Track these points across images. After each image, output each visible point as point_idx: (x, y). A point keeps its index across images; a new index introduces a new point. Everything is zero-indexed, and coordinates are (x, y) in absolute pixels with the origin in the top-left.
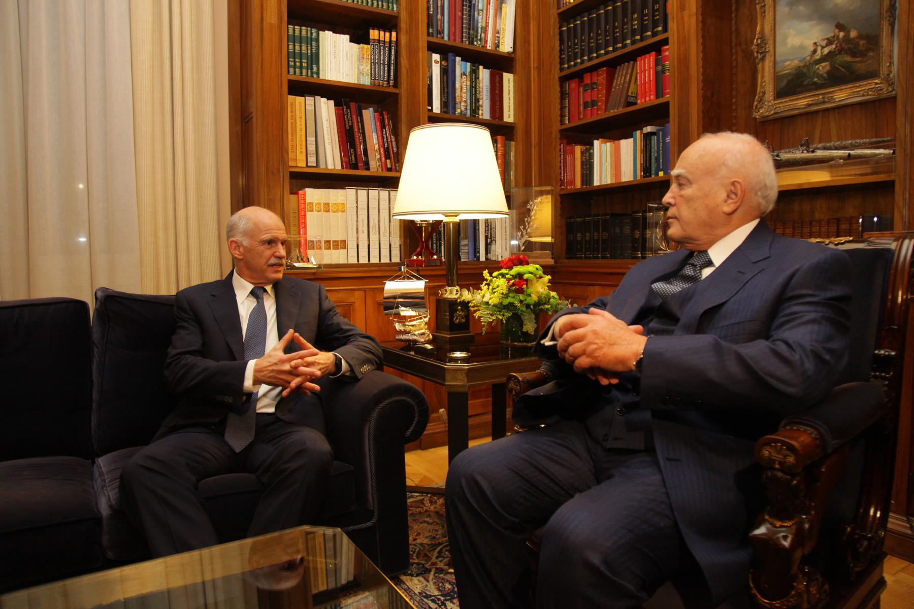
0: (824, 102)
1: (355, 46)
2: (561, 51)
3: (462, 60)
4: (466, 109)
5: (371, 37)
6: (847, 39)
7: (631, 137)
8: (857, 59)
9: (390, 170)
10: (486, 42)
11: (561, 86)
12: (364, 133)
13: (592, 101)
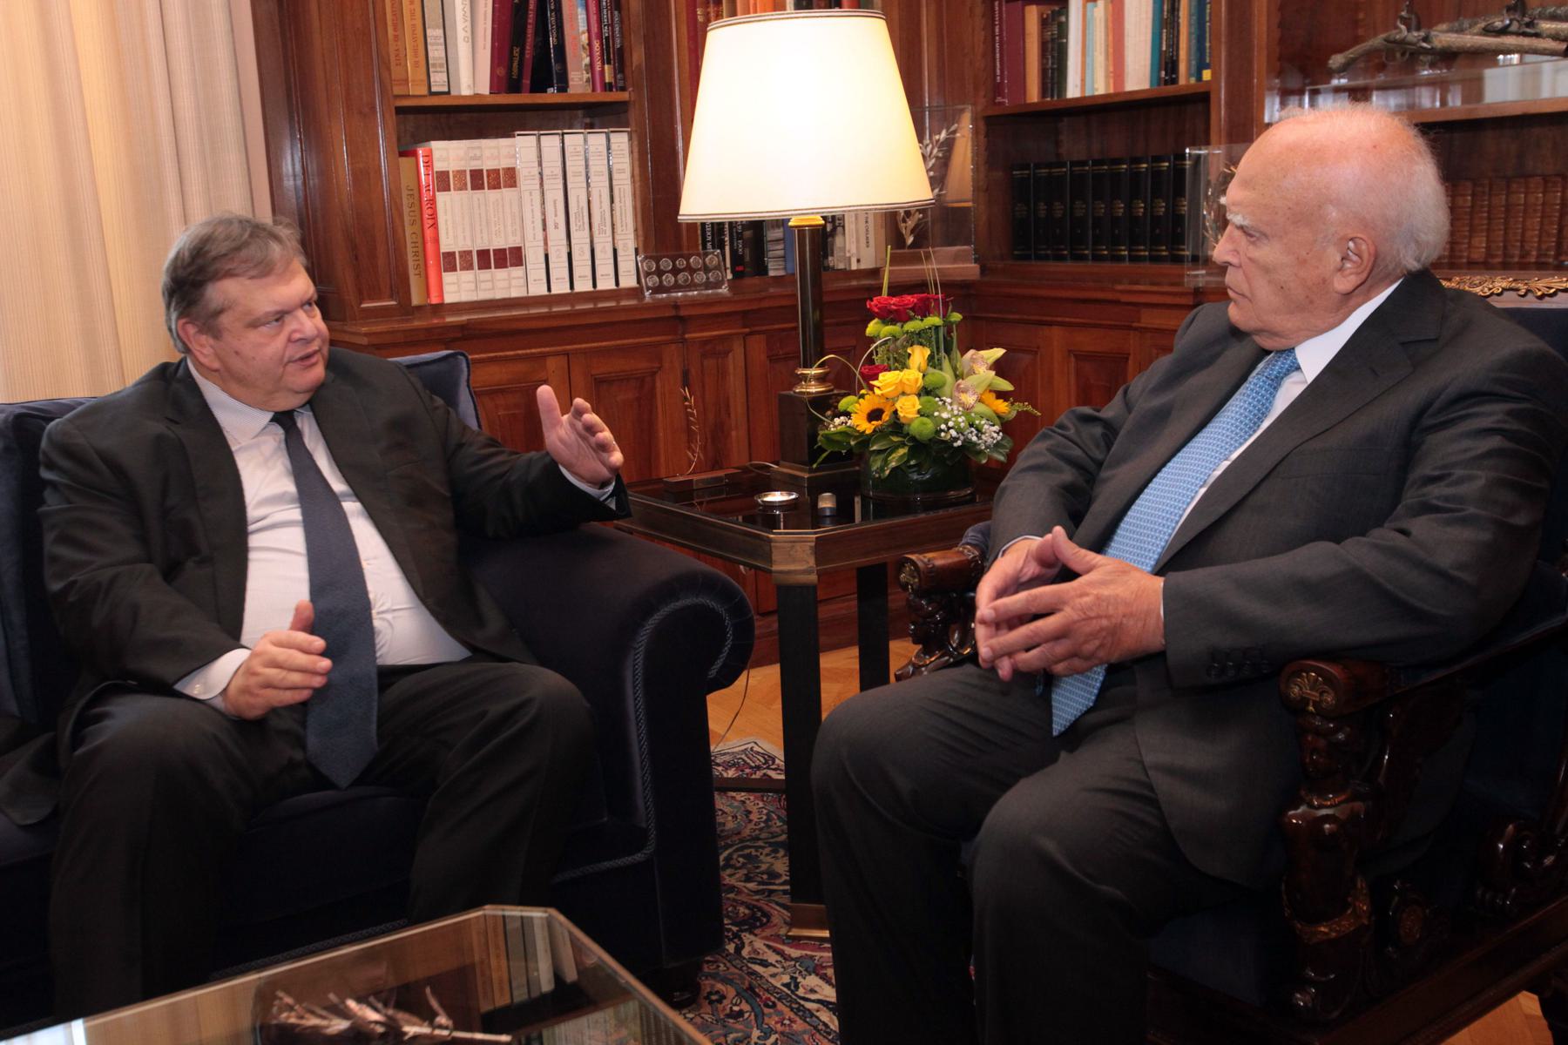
9: (608, 87)
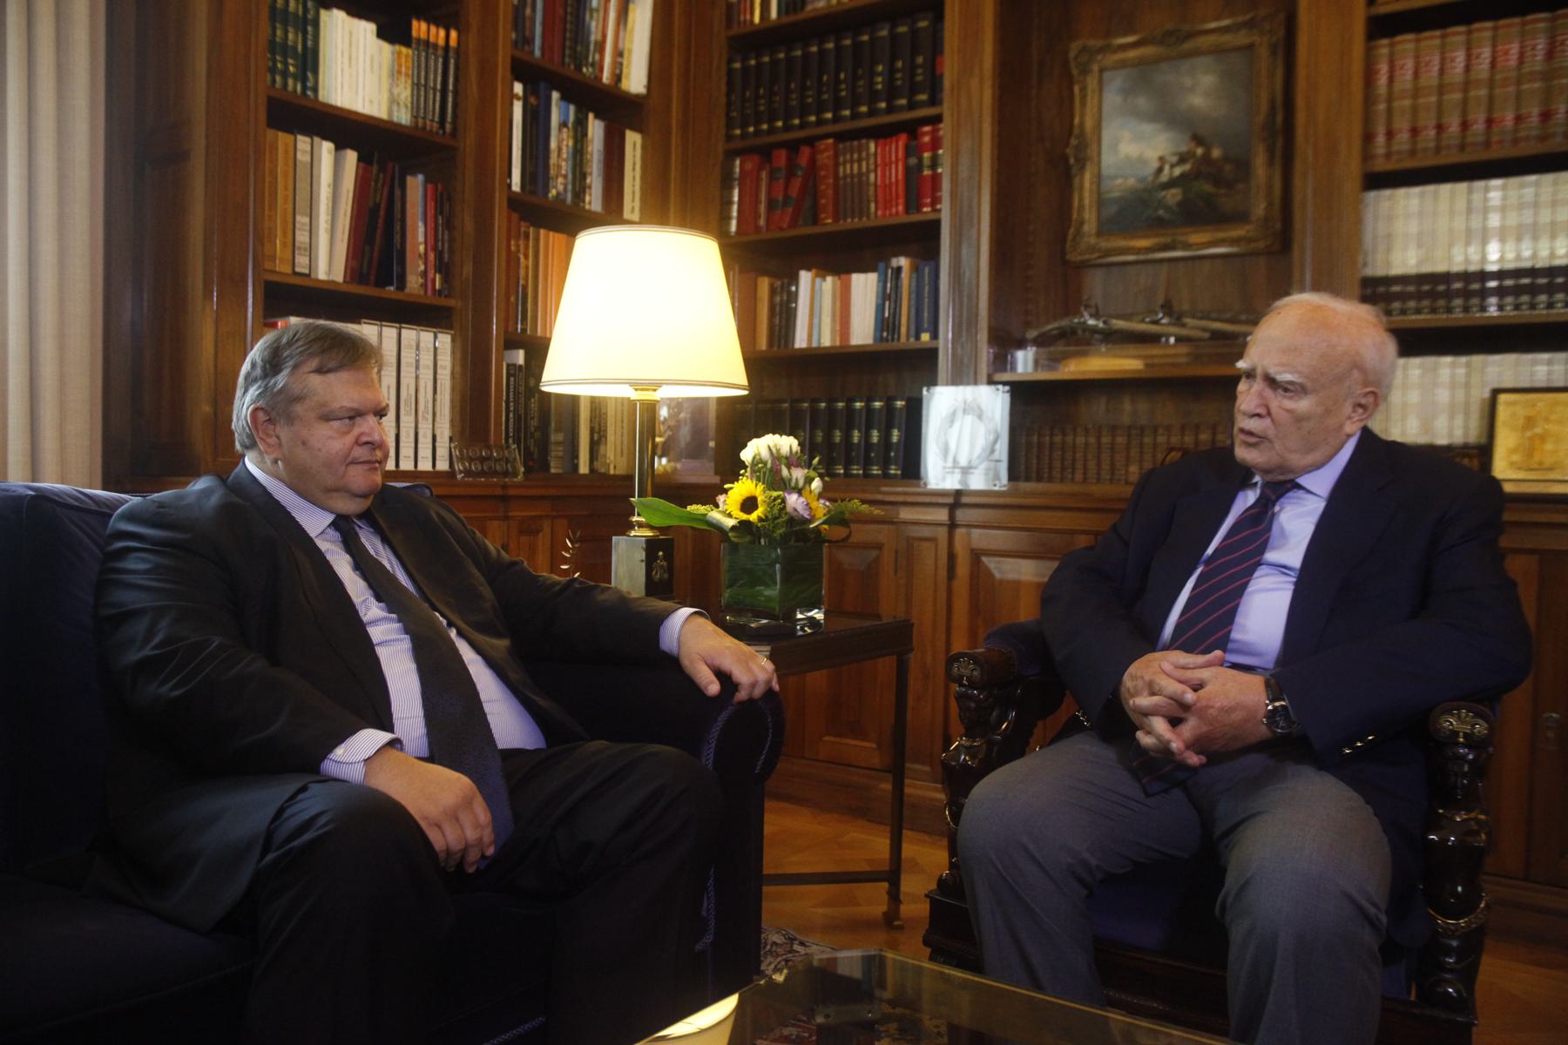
1: (387, 48)
2: (729, 104)
3: (564, 98)
5: (414, 34)
6: (1206, 157)
8: (1223, 191)
10: (601, 70)
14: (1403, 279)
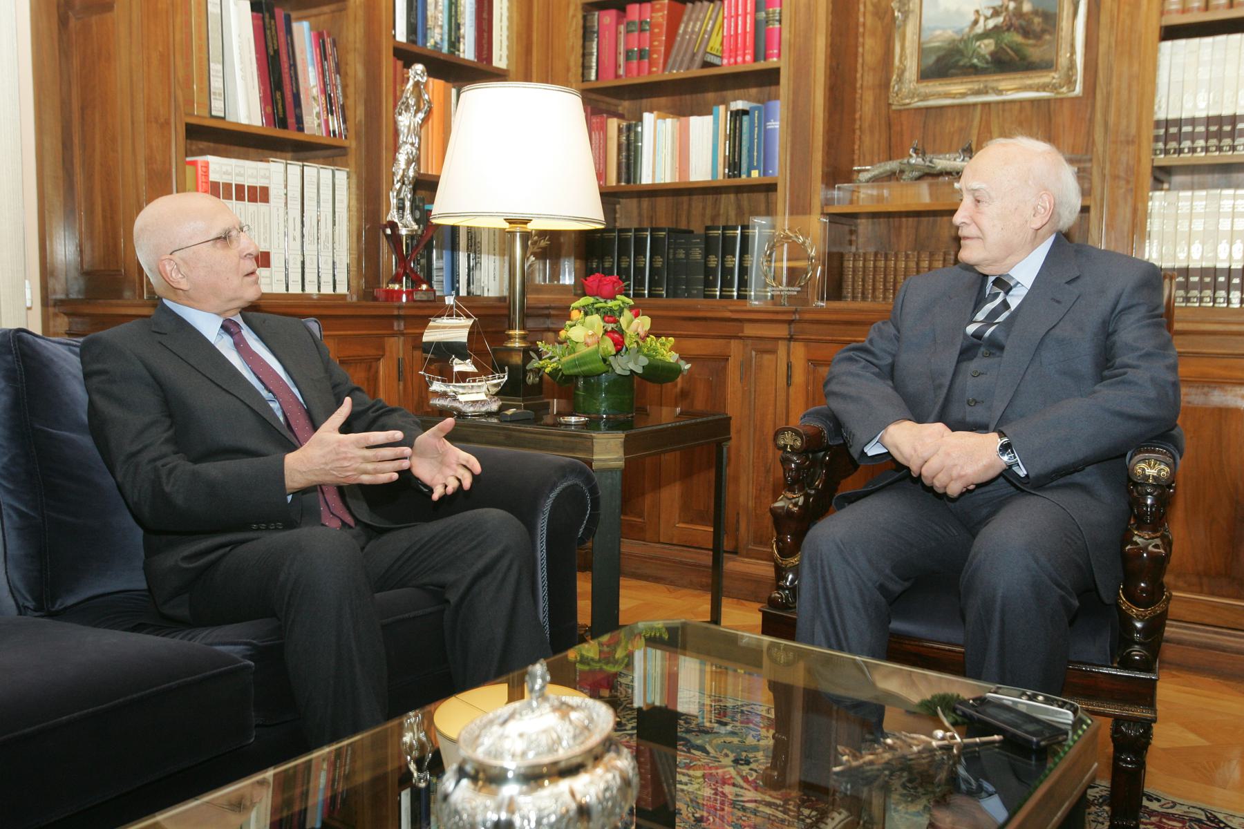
0: (986, 93)
4: (442, 39)
6: (1018, 13)
7: (709, 113)
8: (1031, 42)
11: (585, 18)
12: (293, 65)
13: (641, 51)
14: (1193, 121)
